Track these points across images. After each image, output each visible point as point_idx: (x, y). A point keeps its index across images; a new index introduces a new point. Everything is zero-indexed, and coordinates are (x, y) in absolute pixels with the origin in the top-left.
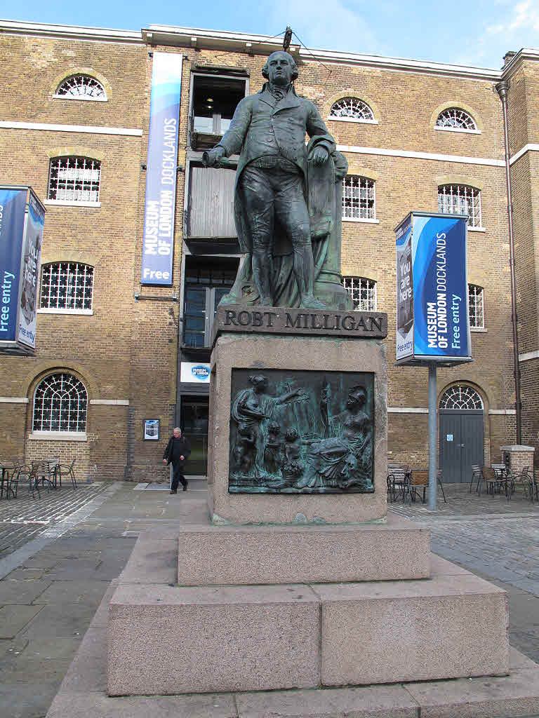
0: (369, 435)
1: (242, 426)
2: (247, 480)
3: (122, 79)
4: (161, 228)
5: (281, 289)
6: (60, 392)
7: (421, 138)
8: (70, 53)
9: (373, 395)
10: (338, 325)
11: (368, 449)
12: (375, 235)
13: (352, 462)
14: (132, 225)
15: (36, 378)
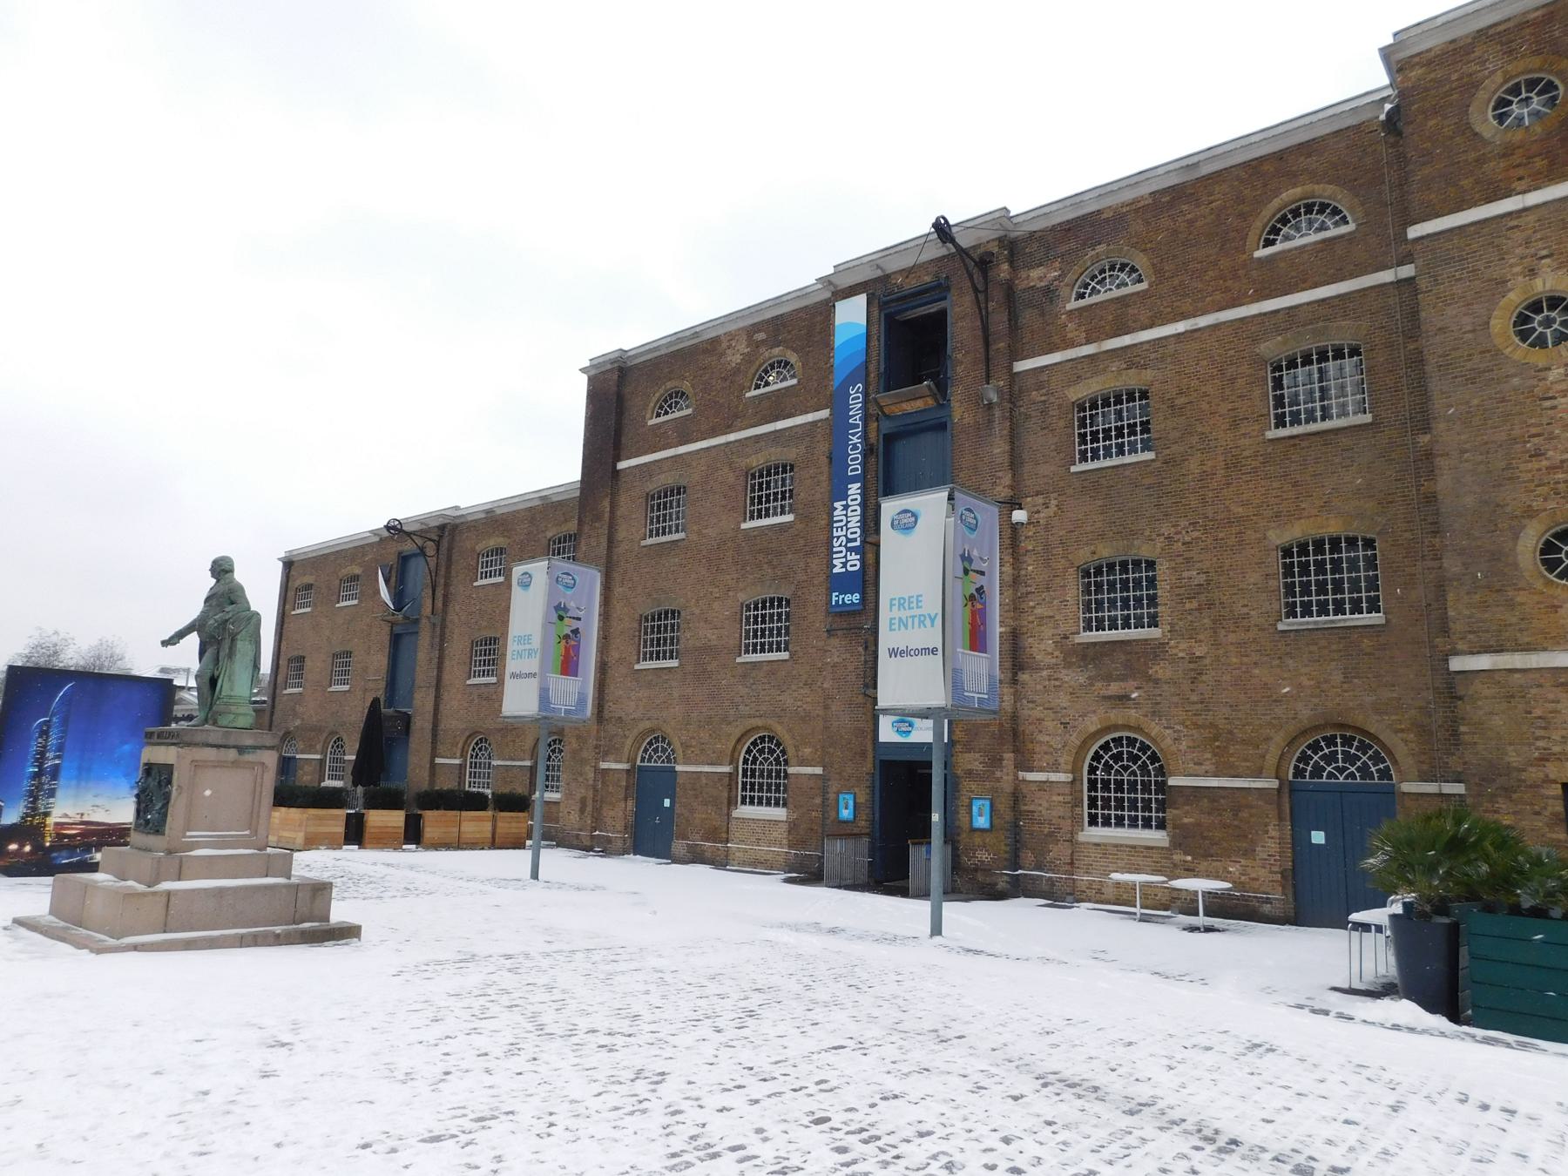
4: (850, 536)
7: (1229, 283)
8: (761, 336)
14: (823, 537)
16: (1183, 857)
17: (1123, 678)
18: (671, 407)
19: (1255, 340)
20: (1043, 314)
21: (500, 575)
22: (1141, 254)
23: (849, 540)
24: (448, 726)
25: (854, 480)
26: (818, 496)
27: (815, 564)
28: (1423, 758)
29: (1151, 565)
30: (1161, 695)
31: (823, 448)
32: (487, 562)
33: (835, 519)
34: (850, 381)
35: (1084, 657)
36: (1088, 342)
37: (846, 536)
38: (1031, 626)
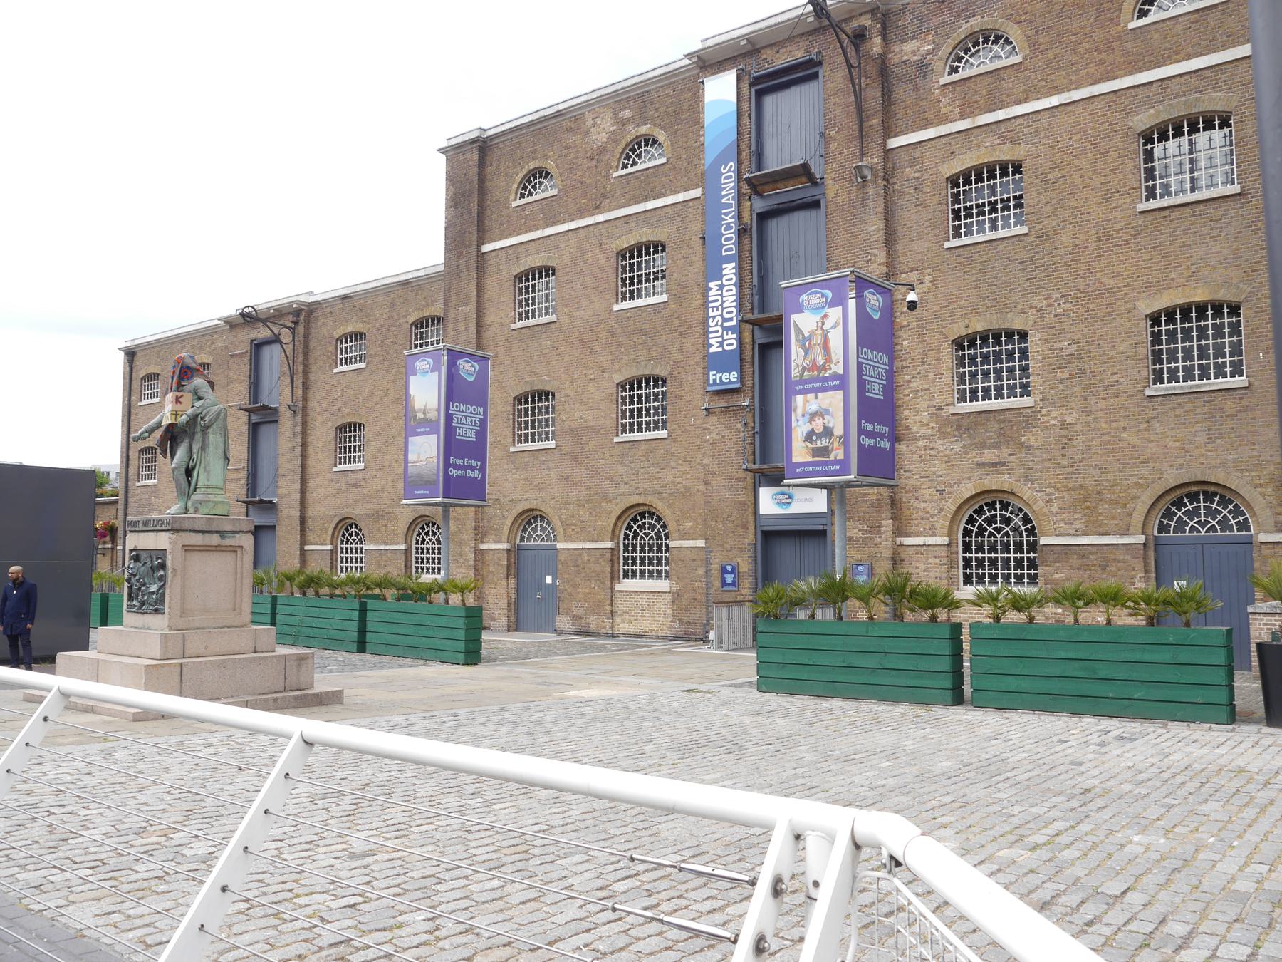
3: (679, 126)
4: (726, 316)
6: (644, 534)
8: (627, 114)
12: (1026, 254)
14: (698, 317)
15: (619, 518)
16: (1054, 610)
17: (996, 446)
18: (534, 187)
19: (1128, 113)
20: (916, 89)
21: (360, 361)
22: (1016, 26)
23: (725, 320)
24: (315, 513)
25: (728, 260)
26: (692, 276)
27: (691, 344)
29: (1023, 336)
30: (1033, 460)
31: (695, 228)
32: (346, 348)
33: (710, 299)
34: (721, 159)
35: (959, 428)
36: (963, 117)
37: (722, 316)
38: (907, 399)
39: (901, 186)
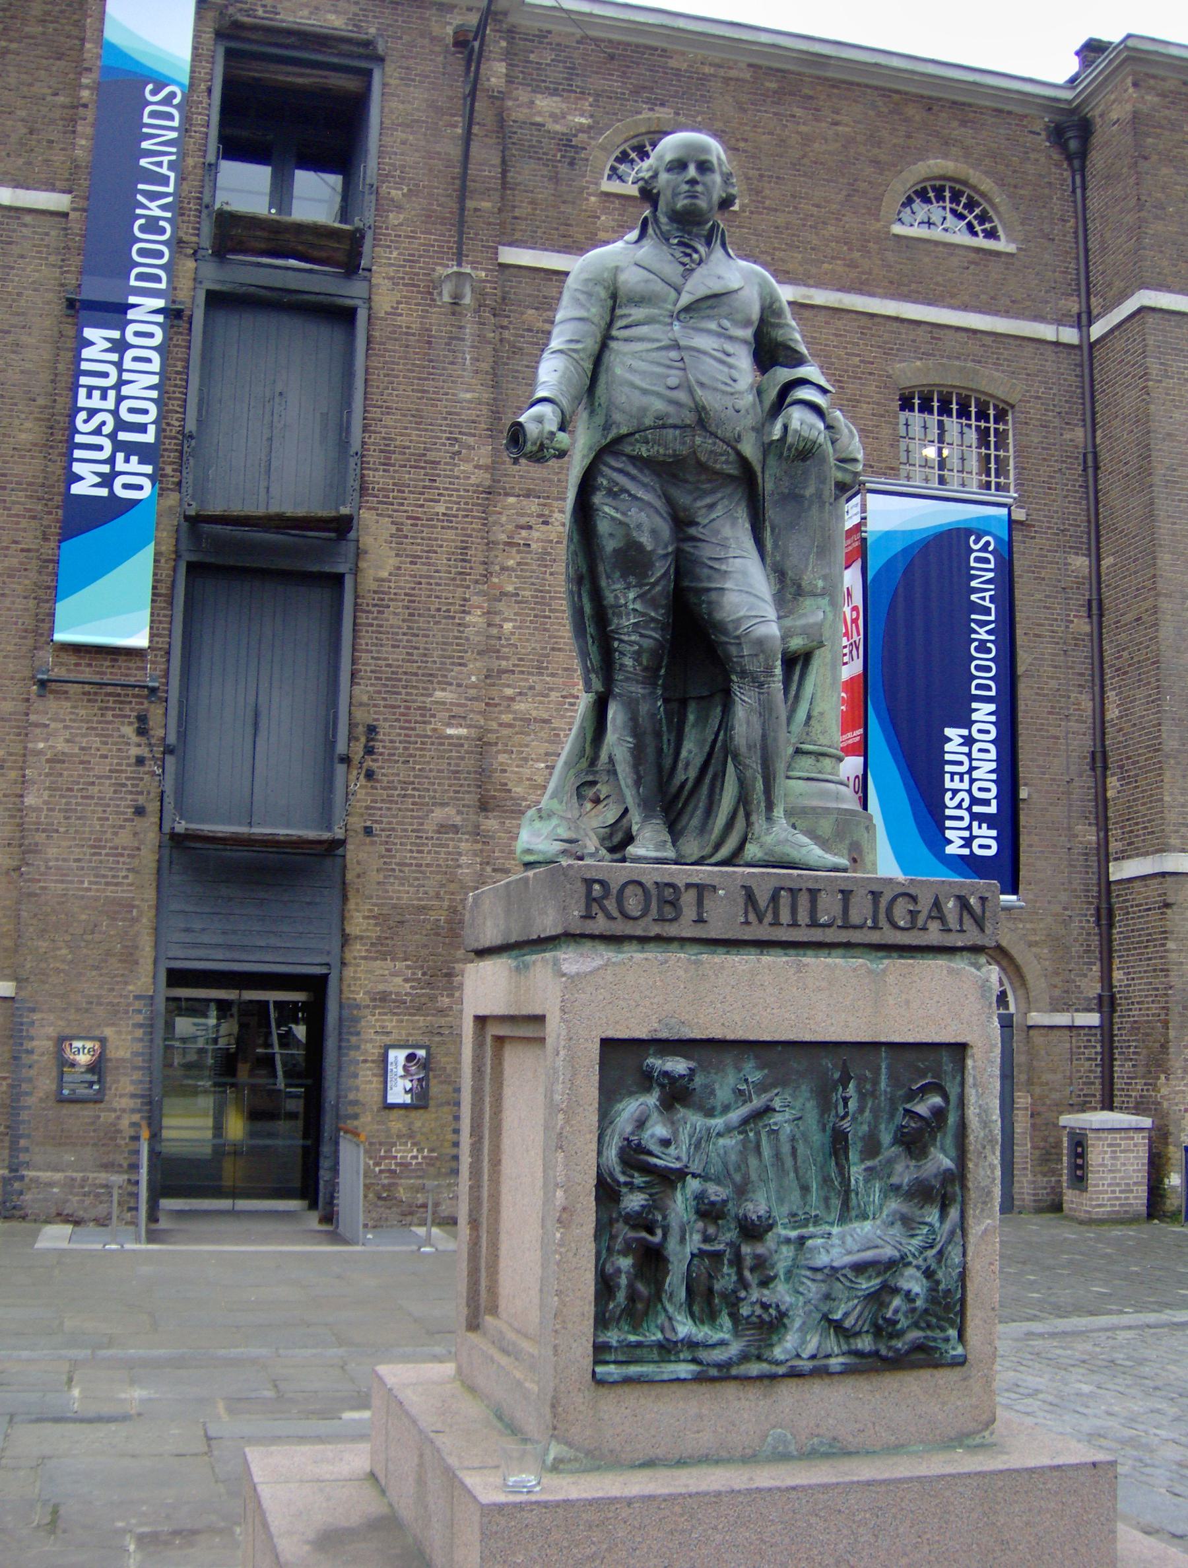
0: (954, 1213)
1: (634, 1201)
2: (639, 1345)
5: (685, 793)
7: (857, 255)
9: (962, 1104)
10: (875, 919)
11: (955, 1255)
13: (916, 1289)
28: (1057, 980)
38: (506, 732)
39: (516, 335)
